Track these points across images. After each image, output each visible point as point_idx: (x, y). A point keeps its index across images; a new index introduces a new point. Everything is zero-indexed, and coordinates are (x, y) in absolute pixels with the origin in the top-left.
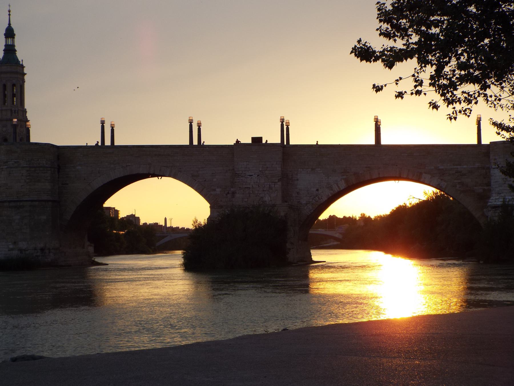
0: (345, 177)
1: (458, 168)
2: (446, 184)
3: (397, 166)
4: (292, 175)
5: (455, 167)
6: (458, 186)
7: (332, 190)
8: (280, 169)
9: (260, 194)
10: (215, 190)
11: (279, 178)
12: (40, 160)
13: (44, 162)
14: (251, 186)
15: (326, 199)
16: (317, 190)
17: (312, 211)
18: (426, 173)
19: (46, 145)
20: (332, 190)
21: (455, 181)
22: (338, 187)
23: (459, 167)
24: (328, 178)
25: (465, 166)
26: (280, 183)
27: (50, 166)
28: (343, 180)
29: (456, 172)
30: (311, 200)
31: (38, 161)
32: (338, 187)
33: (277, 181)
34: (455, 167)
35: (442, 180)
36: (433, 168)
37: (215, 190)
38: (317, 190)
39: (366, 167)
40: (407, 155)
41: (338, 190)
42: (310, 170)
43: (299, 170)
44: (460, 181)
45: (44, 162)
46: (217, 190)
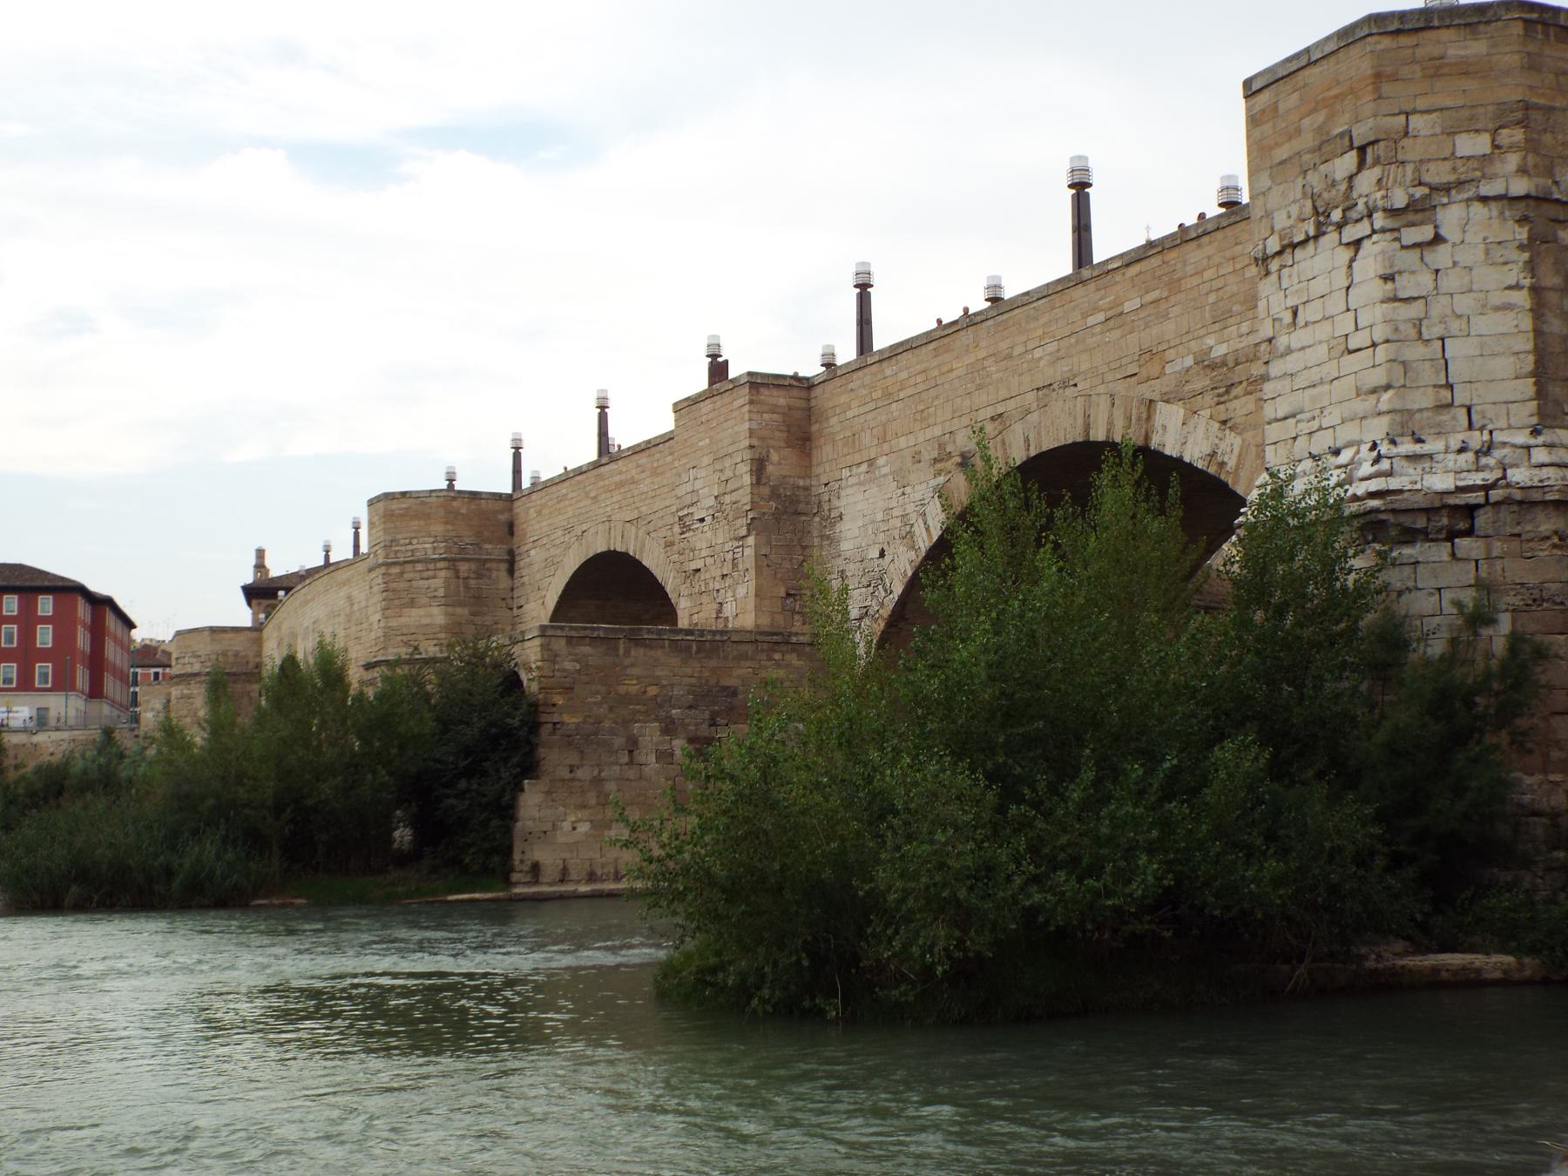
2: (1238, 441)
3: (1075, 385)
4: (830, 500)
8: (747, 479)
9: (718, 590)
11: (751, 515)
12: (415, 541)
13: (427, 546)
16: (882, 554)
18: (1167, 402)
19: (434, 494)
22: (928, 529)
24: (904, 494)
27: (444, 556)
31: (410, 544)
32: (928, 529)
33: (743, 532)
35: (1224, 422)
39: (992, 419)
40: (1101, 317)
42: (864, 467)
45: (427, 546)
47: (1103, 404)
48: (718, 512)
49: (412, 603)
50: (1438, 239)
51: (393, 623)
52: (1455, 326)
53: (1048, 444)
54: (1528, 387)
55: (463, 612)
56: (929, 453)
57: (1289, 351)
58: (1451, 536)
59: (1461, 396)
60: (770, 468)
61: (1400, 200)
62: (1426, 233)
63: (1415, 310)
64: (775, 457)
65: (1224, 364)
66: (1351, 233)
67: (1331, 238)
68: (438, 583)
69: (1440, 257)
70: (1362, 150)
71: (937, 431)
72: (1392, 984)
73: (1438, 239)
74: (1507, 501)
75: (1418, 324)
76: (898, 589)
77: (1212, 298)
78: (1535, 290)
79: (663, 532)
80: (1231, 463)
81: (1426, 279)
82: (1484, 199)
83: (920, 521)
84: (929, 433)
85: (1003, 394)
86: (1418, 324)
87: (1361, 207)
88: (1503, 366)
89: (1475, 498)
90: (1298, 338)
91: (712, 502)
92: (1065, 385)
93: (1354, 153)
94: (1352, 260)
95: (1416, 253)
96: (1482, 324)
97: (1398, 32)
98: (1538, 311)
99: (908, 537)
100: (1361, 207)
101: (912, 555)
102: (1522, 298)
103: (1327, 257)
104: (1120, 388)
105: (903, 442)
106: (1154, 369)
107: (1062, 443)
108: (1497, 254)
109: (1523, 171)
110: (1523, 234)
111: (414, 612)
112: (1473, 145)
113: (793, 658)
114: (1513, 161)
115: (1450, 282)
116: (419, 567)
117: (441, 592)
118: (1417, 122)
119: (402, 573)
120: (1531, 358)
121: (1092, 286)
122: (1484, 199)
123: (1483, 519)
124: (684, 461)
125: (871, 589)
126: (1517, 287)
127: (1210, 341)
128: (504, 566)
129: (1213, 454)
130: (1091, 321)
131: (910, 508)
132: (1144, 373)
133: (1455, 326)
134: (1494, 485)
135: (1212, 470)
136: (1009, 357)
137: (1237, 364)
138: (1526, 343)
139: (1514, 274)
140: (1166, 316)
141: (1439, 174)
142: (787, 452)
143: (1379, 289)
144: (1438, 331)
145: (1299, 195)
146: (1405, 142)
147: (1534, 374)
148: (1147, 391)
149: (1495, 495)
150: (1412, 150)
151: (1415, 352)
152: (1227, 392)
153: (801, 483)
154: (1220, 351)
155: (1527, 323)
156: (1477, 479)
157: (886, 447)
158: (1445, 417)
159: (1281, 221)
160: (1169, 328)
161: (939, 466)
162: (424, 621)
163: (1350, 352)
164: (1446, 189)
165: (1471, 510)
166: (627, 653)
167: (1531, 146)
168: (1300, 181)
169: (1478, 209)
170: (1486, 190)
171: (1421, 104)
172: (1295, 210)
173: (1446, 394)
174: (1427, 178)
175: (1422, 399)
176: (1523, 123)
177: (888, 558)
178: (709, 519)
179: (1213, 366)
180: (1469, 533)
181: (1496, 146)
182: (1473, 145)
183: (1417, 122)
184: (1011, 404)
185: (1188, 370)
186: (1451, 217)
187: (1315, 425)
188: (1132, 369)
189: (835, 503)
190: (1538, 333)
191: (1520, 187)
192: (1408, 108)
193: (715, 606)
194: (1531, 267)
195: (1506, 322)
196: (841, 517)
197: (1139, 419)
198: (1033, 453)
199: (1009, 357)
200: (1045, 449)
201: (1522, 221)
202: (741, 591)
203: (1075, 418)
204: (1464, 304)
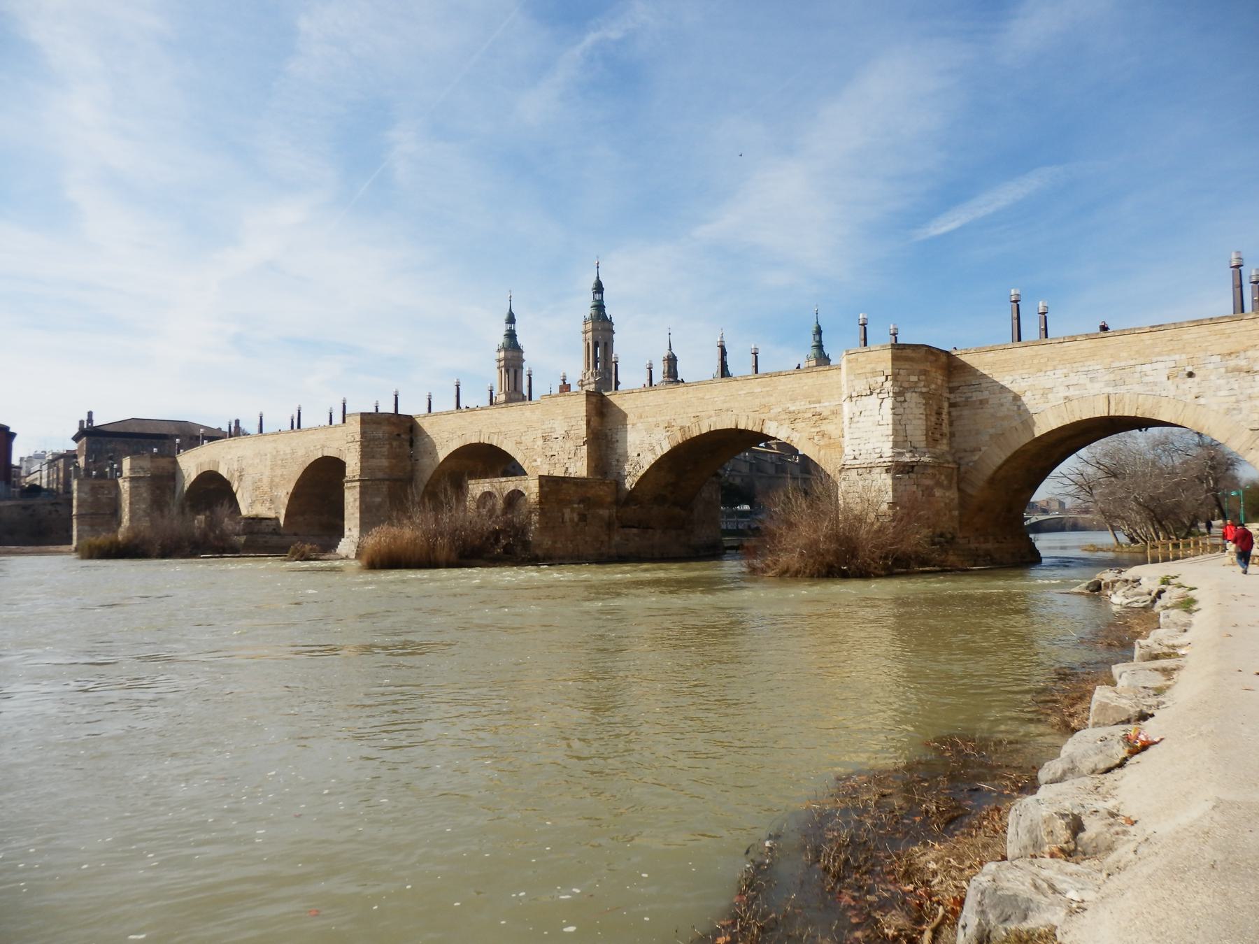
0: (669, 433)
1: (815, 407)
2: (798, 435)
4: (612, 435)
5: (812, 406)
6: (816, 438)
7: (655, 454)
8: (585, 427)
10: (535, 461)
14: (556, 453)
15: (648, 467)
16: (639, 455)
17: (633, 486)
20: (655, 454)
21: (813, 430)
22: (662, 449)
23: (817, 405)
25: (827, 404)
26: (586, 447)
28: (667, 439)
29: (813, 415)
30: (631, 470)
32: (662, 449)
33: (582, 444)
34: (812, 406)
36: (780, 410)
37: (535, 461)
38: (639, 455)
40: (744, 392)
41: (662, 454)
43: (619, 427)
44: (818, 429)
46: (539, 460)
47: (745, 418)
48: (567, 436)
49: (373, 457)
50: (905, 401)
51: (365, 464)
52: (908, 422)
53: (719, 428)
54: (924, 438)
55: (394, 461)
56: (662, 426)
57: (858, 422)
58: (908, 473)
59: (909, 439)
60: (591, 423)
61: (897, 391)
62: (902, 399)
63: (899, 417)
64: (593, 419)
65: (794, 412)
66: (880, 396)
67: (875, 395)
68: (385, 449)
69: (906, 405)
70: (887, 376)
71: (668, 418)
72: (968, 570)
73: (905, 401)
74: (922, 465)
75: (900, 421)
76: (647, 467)
77: (790, 393)
78: (926, 415)
79: (515, 438)
80: (796, 440)
81: (902, 410)
82: (916, 392)
83: (659, 446)
84: (663, 418)
85: (700, 409)
86: (900, 421)
87: (886, 389)
88: (919, 432)
89: (915, 464)
90: (862, 419)
91: (563, 432)
92: (727, 410)
93: (884, 378)
94: (882, 402)
95: (899, 404)
96: (914, 422)
97: (898, 349)
98: (926, 420)
99: (653, 450)
100: (886, 389)
101: (654, 456)
102: (923, 417)
103: (874, 400)
104: (752, 415)
105: (650, 420)
106: (767, 410)
107: (725, 428)
108: (919, 406)
109: (924, 386)
110: (924, 402)
111: (374, 460)
112: (914, 378)
113: (605, 488)
114: (922, 384)
115: (908, 411)
116: (376, 443)
117: (386, 453)
118: (901, 372)
119: (369, 445)
120: (925, 431)
121: (740, 382)
122: (916, 392)
123: (916, 469)
124: (546, 417)
125: (633, 466)
126: (922, 414)
127: (789, 405)
128: (408, 444)
129: (788, 438)
130: (739, 393)
131: (654, 441)
132: (762, 411)
133: (908, 422)
134: (919, 461)
135: (788, 442)
136: (703, 399)
137: (799, 413)
138: (924, 428)
139: (922, 411)
140: (772, 395)
141: (906, 385)
142: (596, 418)
143: (891, 412)
144: (904, 423)
145: (865, 383)
146: (899, 376)
147: (926, 435)
148: (763, 417)
149: (919, 464)
150: (900, 378)
151: (899, 427)
152: (795, 420)
153: (600, 428)
154: (792, 409)
155: (924, 423)
156: (913, 459)
157: (642, 420)
158: (905, 444)
159: (857, 389)
160: (772, 399)
161: (667, 429)
162: (379, 464)
163: (879, 425)
164: (907, 389)
165: (913, 467)
166: (562, 485)
167: (926, 380)
168: (865, 380)
169: (914, 394)
170: (916, 390)
171: (903, 367)
172: (863, 387)
173: (906, 438)
174: (903, 385)
175: (900, 439)
176: (925, 375)
177: (641, 457)
178: (561, 438)
179: (790, 413)
180: (912, 472)
181: (919, 380)
182: (914, 378)
183: (901, 372)
184: (703, 414)
185: (779, 412)
186: (908, 395)
187: (867, 442)
188: (758, 409)
189: (614, 436)
190: (927, 425)
191: (924, 390)
192: (899, 367)
193: (564, 469)
194: (925, 409)
195: (920, 422)
196: (617, 441)
197: (759, 424)
198: (712, 429)
199: (703, 399)
200: (718, 428)
201: (924, 398)
202: (579, 464)
203: (732, 421)
204: (910, 417)
